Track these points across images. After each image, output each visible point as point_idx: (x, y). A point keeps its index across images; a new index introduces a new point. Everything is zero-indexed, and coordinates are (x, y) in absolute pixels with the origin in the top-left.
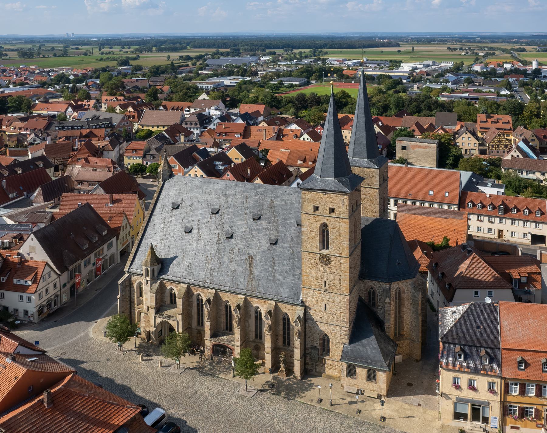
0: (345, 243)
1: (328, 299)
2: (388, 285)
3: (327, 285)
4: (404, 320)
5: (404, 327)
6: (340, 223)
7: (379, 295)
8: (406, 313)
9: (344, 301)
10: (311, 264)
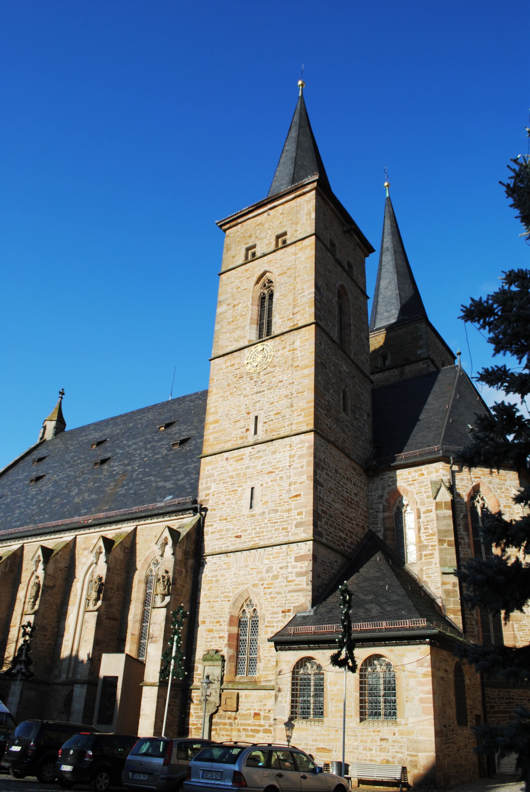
1: (259, 468)
9: (300, 457)
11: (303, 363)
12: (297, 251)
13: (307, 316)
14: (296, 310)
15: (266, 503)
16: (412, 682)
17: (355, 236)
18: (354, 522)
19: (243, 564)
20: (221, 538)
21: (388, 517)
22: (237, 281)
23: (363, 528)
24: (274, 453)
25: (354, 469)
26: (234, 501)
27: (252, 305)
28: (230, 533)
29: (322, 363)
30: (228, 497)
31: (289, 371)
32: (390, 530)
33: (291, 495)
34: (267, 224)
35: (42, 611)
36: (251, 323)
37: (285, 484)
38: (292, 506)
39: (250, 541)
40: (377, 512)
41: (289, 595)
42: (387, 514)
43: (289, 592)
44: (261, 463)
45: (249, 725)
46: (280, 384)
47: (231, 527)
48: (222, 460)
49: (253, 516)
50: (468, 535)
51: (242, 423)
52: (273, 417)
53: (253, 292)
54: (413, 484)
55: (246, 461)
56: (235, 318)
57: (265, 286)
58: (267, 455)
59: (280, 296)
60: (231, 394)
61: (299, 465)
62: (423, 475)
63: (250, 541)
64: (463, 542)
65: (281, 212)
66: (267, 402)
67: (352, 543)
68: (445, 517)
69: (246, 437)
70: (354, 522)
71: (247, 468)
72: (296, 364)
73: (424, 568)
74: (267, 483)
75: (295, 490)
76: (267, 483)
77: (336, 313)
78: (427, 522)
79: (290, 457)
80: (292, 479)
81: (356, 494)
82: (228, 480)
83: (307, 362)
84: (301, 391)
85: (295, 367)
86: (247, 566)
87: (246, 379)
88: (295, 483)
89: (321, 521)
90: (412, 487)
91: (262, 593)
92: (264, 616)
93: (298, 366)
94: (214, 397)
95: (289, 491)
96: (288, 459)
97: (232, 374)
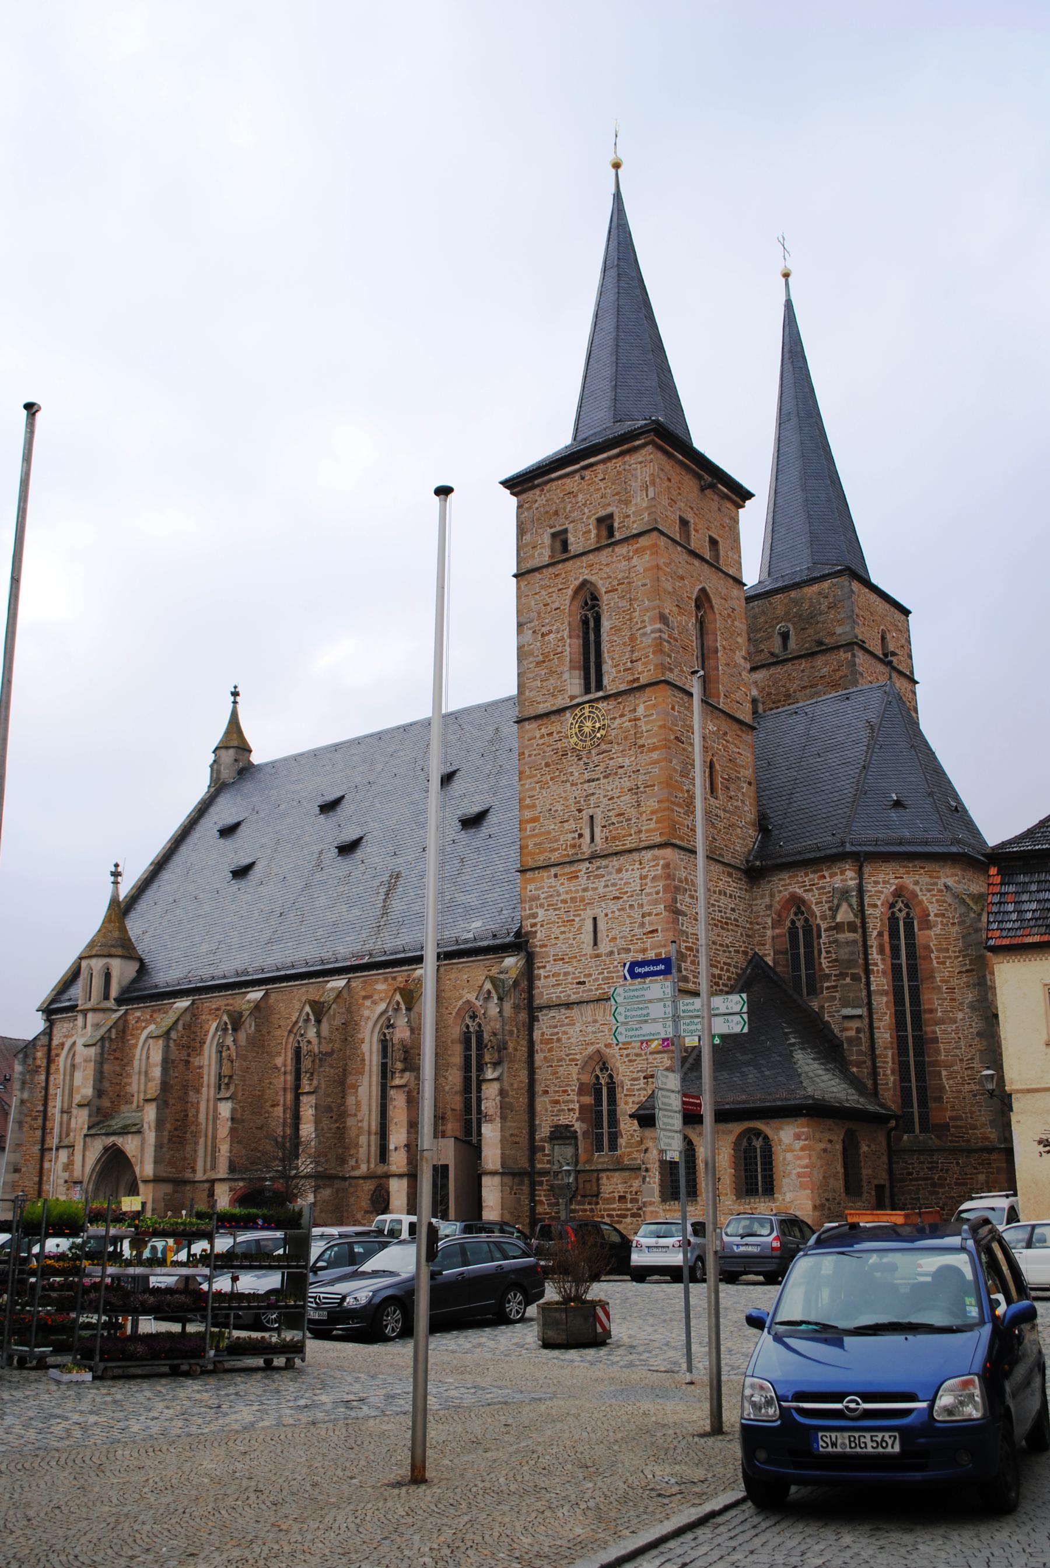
0: (648, 629)
1: (601, 890)
2: (850, 874)
3: (597, 830)
4: (938, 1052)
5: (942, 1088)
6: (629, 559)
7: (823, 926)
8: (941, 1022)
9: (654, 878)
10: (547, 765)
11: (649, 741)
12: (631, 554)
13: (652, 668)
15: (614, 939)
16: (789, 1156)
17: (720, 486)
18: (731, 949)
19: (590, 1019)
20: (558, 985)
21: (779, 936)
22: (543, 593)
23: (745, 953)
24: (619, 871)
25: (730, 875)
26: (571, 935)
27: (570, 637)
28: (570, 977)
29: (677, 738)
30: (563, 929)
31: (631, 752)
32: (782, 953)
33: (645, 930)
34: (580, 497)
35: (323, 1086)
36: (571, 668)
37: (637, 914)
38: (648, 945)
39: (597, 989)
40: (764, 928)
41: (651, 1057)
42: (777, 931)
43: (651, 1053)
44: (603, 884)
45: (614, 1209)
46: (620, 771)
47: (570, 969)
48: (549, 877)
49: (598, 956)
50: (883, 960)
51: (571, 825)
52: (614, 820)
53: (570, 615)
54: (811, 890)
55: (583, 881)
57: (586, 604)
58: (610, 873)
60: (552, 779)
61: (654, 890)
62: (824, 877)
63: (597, 989)
64: (875, 968)
65: (601, 476)
66: (605, 796)
67: (729, 979)
68: (847, 943)
69: (580, 846)
70: (731, 949)
71: (585, 890)
72: (640, 742)
73: (826, 1005)
74: (613, 912)
75: (650, 924)
76: (613, 912)
77: (694, 644)
78: (830, 943)
79: (641, 879)
80: (646, 909)
81: (733, 910)
82: (560, 905)
83: (655, 740)
84: (649, 783)
85: (640, 747)
86: (595, 1021)
87: (571, 758)
88: (650, 914)
89: (685, 962)
90: (810, 894)
91: (617, 1055)
92: (622, 1082)
93: (644, 746)
94: (528, 781)
95: (642, 925)
96: (638, 881)
97: (550, 748)
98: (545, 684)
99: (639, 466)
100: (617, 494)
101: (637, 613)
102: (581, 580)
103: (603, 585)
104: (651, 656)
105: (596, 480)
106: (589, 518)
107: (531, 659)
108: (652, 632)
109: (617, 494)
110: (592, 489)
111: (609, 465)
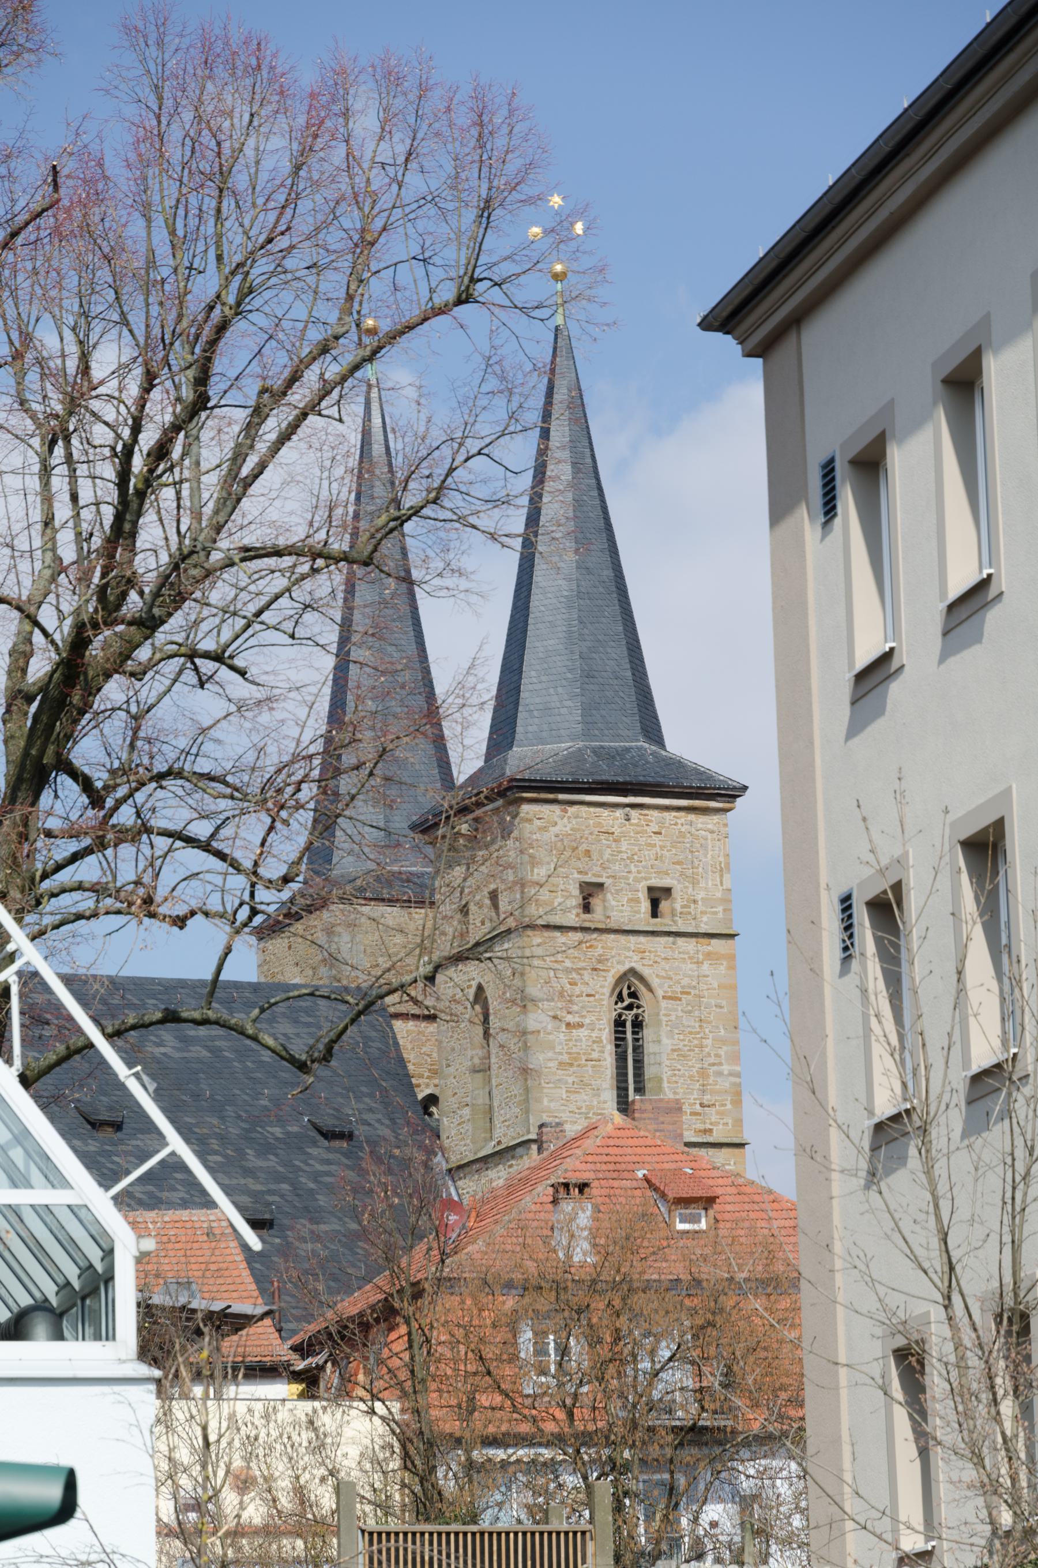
0: (726, 1068)
12: (701, 957)
13: (730, 1122)
14: (707, 1098)
34: (624, 846)
56: (576, 1059)
59: (673, 1050)
98: (572, 1097)
99: (710, 836)
100: (678, 863)
101: (709, 1042)
102: (627, 967)
103: (661, 986)
104: (729, 1106)
105: (648, 829)
106: (637, 880)
107: (550, 1054)
108: (731, 1074)
109: (678, 863)
110: (642, 841)
111: (666, 815)
